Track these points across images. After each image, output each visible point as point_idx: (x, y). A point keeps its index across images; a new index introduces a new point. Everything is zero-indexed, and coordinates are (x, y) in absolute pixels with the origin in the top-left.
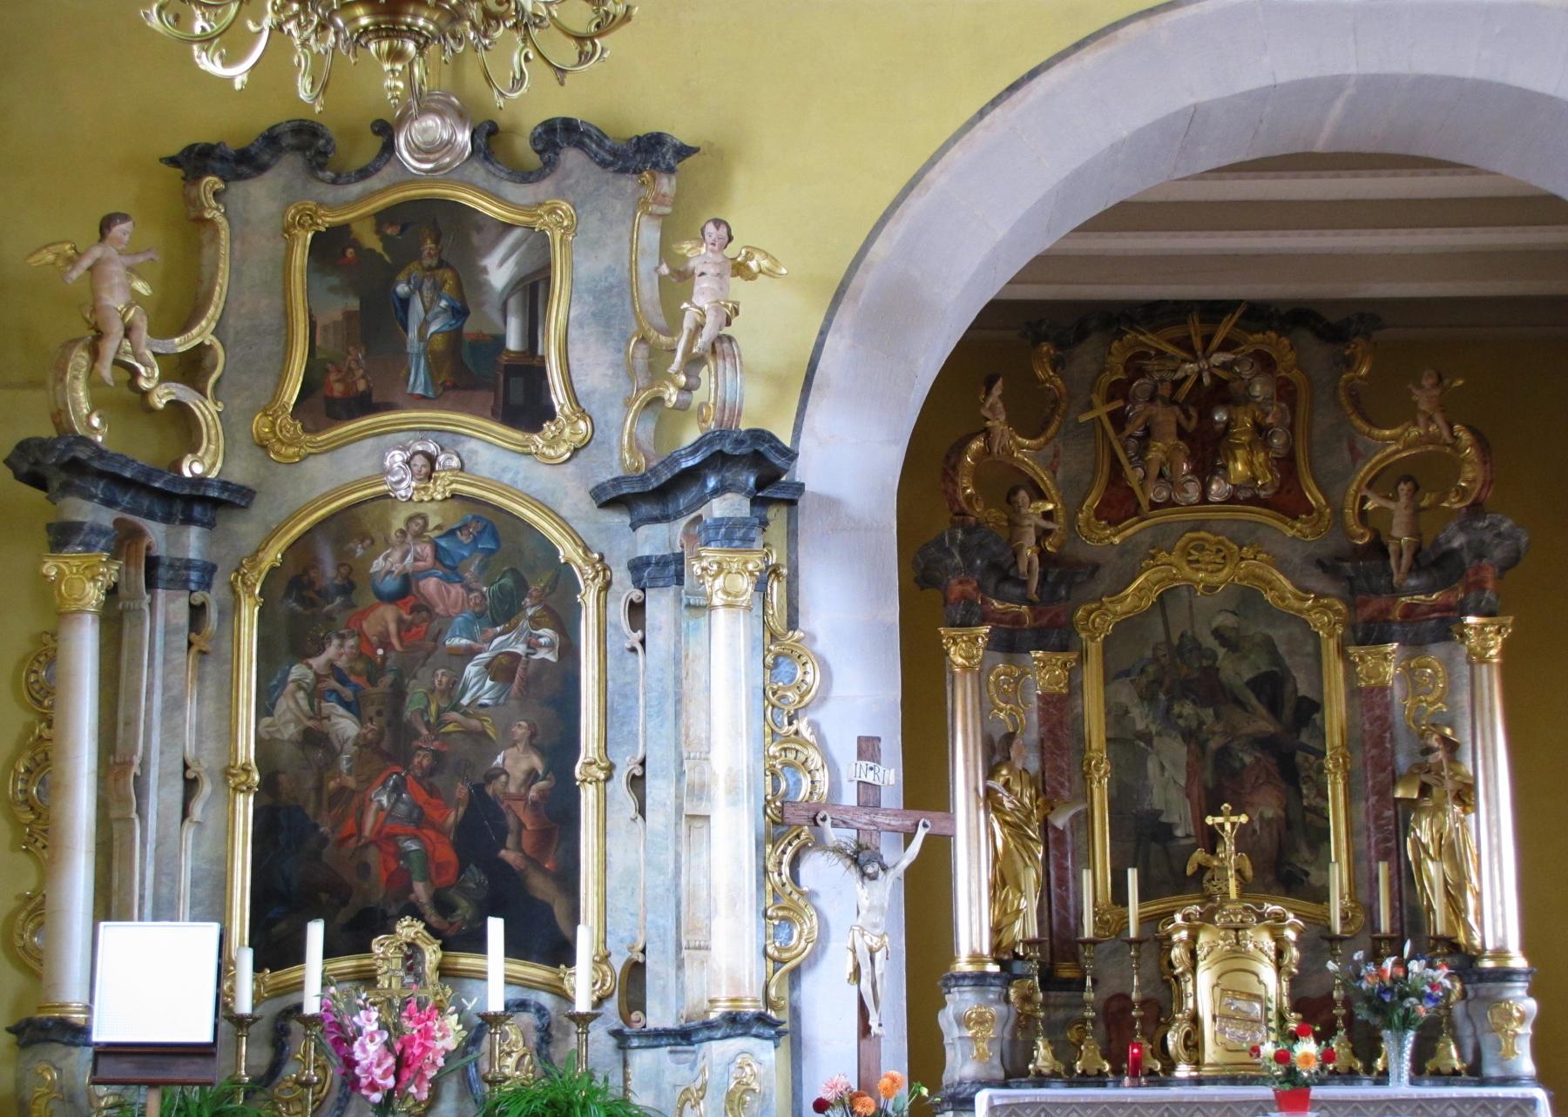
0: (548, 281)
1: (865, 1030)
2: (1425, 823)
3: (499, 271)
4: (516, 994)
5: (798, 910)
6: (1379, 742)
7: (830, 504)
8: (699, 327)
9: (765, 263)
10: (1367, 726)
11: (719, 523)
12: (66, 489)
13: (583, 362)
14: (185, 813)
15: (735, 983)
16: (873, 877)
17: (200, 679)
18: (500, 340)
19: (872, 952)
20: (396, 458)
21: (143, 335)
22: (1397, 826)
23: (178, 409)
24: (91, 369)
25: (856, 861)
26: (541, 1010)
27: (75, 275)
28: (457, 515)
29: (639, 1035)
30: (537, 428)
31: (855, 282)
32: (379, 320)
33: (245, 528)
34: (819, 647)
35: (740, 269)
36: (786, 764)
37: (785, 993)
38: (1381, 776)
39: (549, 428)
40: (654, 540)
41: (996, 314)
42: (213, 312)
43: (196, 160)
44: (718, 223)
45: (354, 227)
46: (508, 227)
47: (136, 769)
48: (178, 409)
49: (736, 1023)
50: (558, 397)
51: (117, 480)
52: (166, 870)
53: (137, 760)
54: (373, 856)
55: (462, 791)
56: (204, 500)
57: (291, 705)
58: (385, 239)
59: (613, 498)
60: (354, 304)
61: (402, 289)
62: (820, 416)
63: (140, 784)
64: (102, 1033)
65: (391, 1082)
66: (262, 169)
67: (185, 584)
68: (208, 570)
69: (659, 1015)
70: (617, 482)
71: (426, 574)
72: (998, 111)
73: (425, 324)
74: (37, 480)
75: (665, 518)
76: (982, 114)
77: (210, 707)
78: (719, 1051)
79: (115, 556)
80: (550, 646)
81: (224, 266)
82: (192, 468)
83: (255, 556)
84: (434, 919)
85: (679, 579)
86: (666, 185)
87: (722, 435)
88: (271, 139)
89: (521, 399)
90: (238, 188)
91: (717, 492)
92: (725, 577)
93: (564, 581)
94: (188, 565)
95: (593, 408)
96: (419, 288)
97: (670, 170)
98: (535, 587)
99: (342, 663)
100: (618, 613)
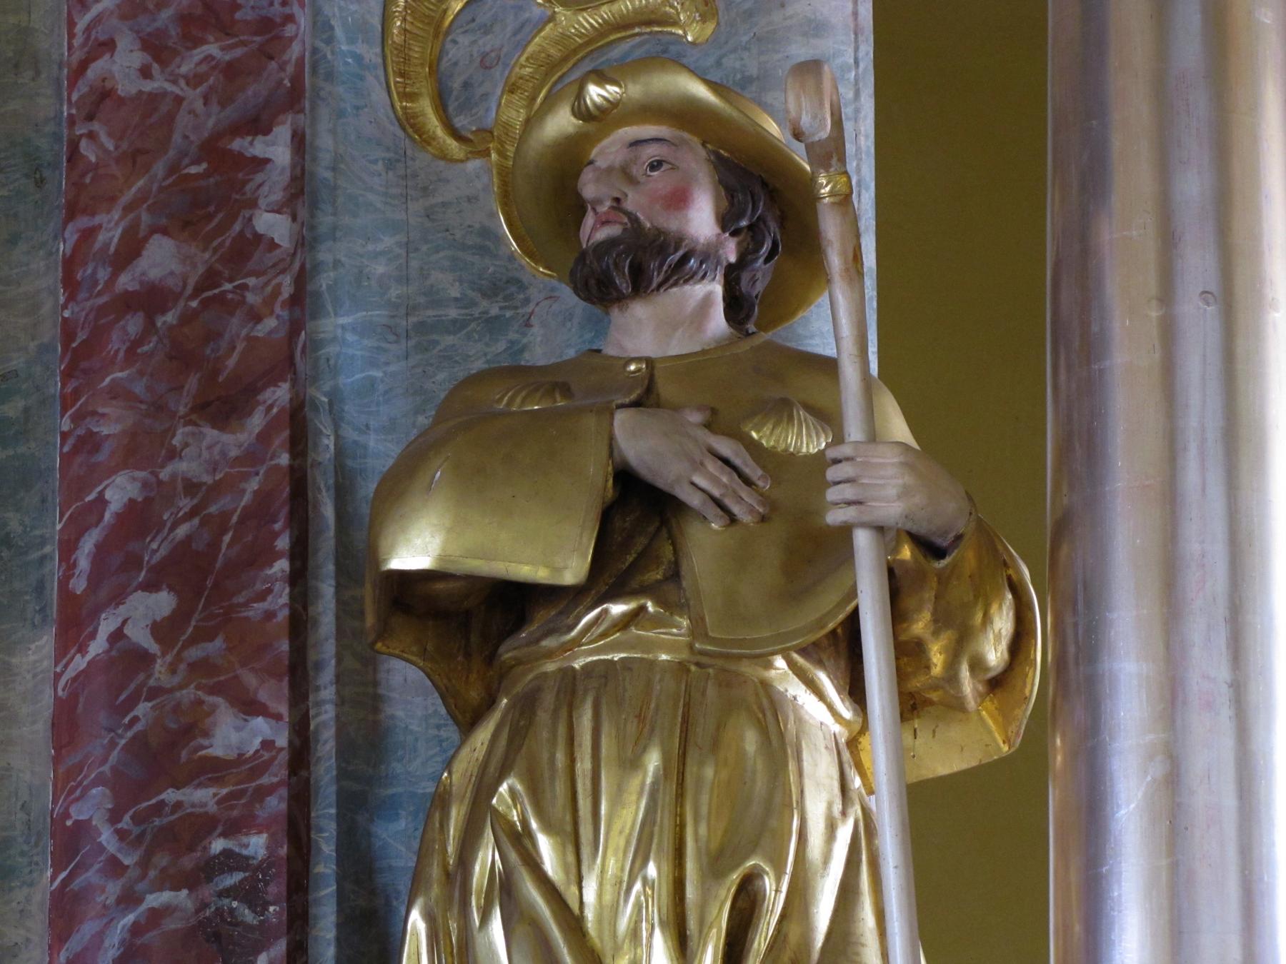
2: (624, 813)
6: (209, 196)
10: (123, 66)
22: (297, 831)
38: (201, 451)
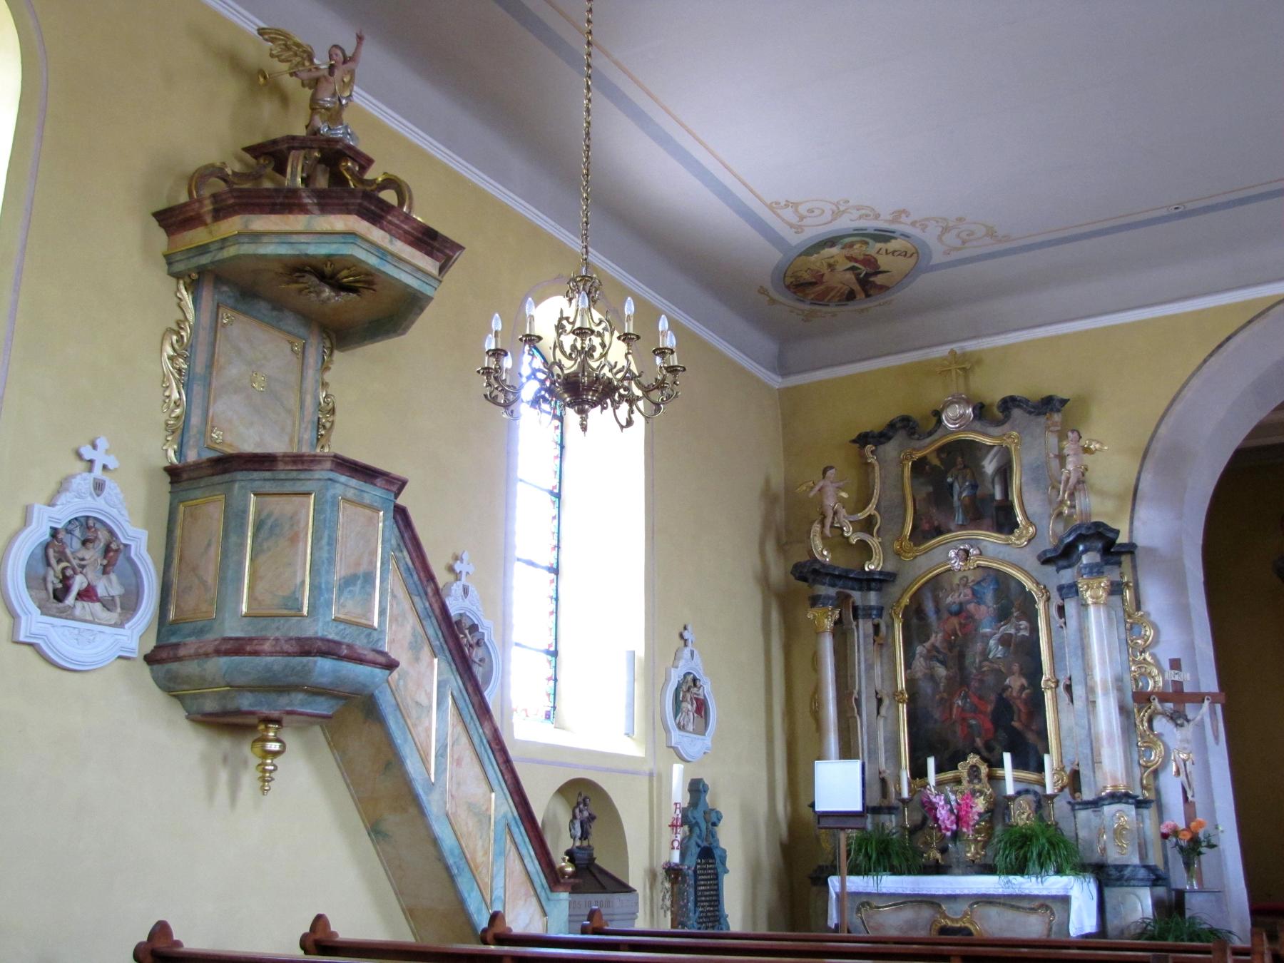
0: (1011, 467)
1: (1186, 799)
3: (989, 466)
4: (1022, 787)
5: (1155, 744)
7: (1150, 551)
8: (1068, 479)
9: (1098, 446)
11: (1086, 566)
12: (815, 582)
13: (1028, 502)
14: (878, 713)
15: (1114, 778)
16: (1182, 726)
17: (881, 656)
18: (993, 496)
19: (1185, 761)
20: (952, 554)
21: (843, 512)
23: (862, 543)
24: (822, 532)
25: (1171, 718)
26: (1036, 793)
27: (812, 494)
28: (979, 575)
29: (1079, 804)
30: (1011, 532)
31: (1152, 448)
32: (941, 496)
33: (894, 590)
34: (1153, 617)
35: (1087, 450)
36: (1141, 674)
37: (1151, 782)
39: (1017, 531)
40: (1067, 576)
41: (1239, 454)
42: (874, 501)
43: (863, 439)
44: (1073, 431)
45: (929, 457)
46: (992, 447)
47: (855, 695)
48: (862, 543)
49: (1115, 798)
50: (1020, 518)
51: (834, 576)
52: (872, 738)
53: (855, 692)
54: (958, 728)
55: (993, 697)
56: (875, 580)
57: (919, 663)
58: (941, 460)
59: (1046, 561)
60: (930, 489)
61: (949, 480)
62: (1143, 512)
63: (858, 702)
64: (820, 807)
65: (954, 827)
66: (890, 439)
67: (868, 616)
68: (880, 610)
69: (1087, 794)
70: (1045, 552)
71: (969, 602)
72: (1213, 359)
73: (960, 493)
74: (805, 579)
75: (1069, 566)
76: (1205, 361)
77: (886, 667)
78: (1108, 810)
79: (835, 607)
80: (1025, 629)
81: (878, 481)
82: (869, 567)
83: (898, 602)
84: (985, 754)
85: (1077, 592)
86: (1057, 417)
87: (1080, 526)
88: (892, 426)
89: (1004, 521)
90: (881, 448)
91: (1085, 551)
92: (1094, 592)
93: (1029, 600)
94: (871, 608)
95: (1036, 521)
96: (957, 478)
97: (1058, 411)
98: (1016, 603)
99: (938, 644)
100: (1054, 611)
